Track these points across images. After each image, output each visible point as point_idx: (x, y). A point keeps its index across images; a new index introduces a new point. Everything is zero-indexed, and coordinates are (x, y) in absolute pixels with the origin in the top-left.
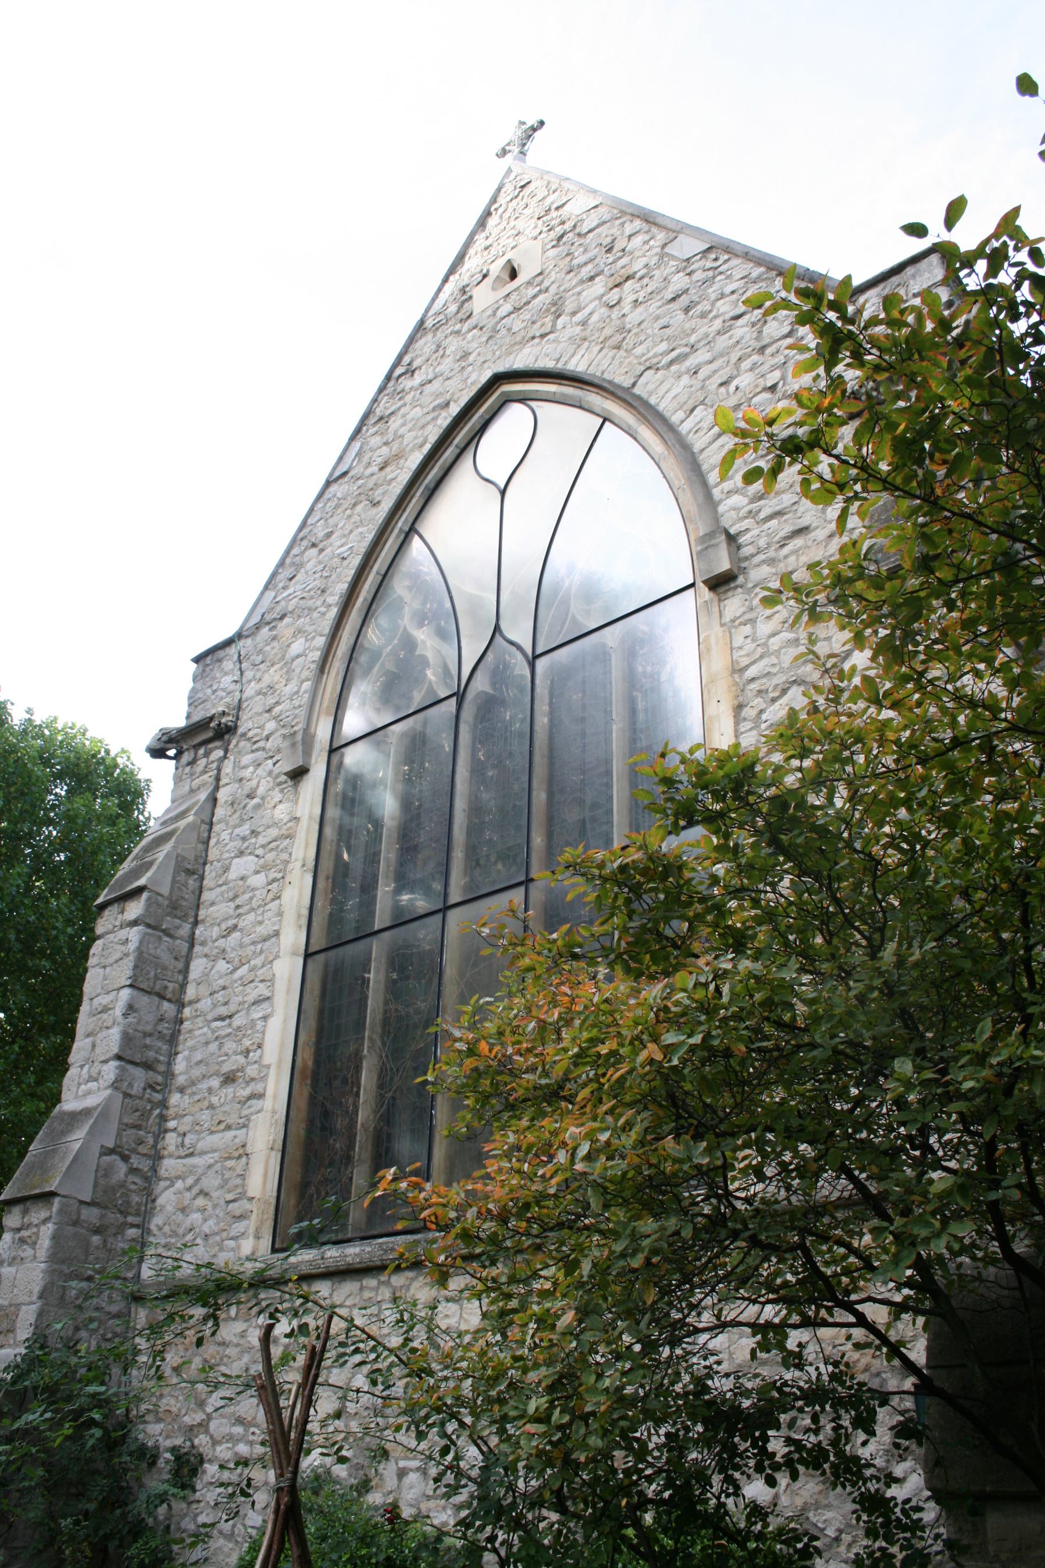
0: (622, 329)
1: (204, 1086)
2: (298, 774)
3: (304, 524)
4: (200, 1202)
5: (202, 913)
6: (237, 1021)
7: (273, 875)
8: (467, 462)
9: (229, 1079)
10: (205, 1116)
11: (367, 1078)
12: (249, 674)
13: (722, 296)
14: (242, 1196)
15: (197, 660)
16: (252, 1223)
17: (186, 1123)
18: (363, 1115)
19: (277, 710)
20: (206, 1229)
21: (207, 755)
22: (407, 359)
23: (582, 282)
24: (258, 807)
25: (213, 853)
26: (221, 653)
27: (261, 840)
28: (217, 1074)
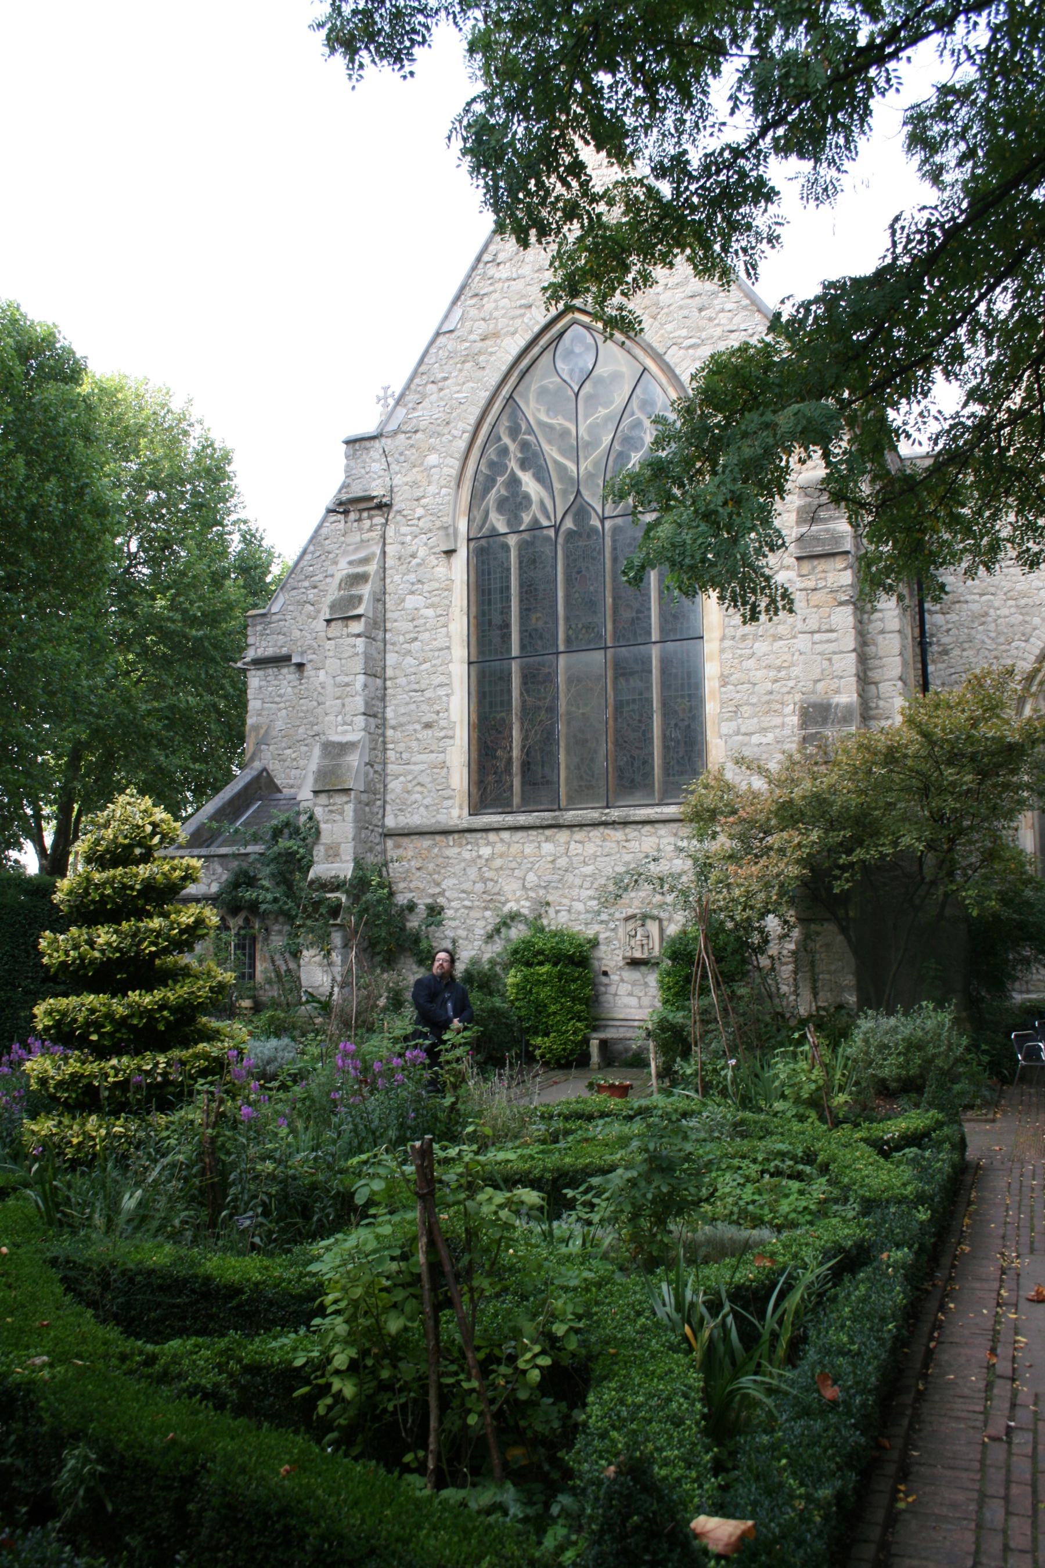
0: (656, 304)
1: (410, 727)
2: (450, 553)
3: (421, 362)
4: (419, 788)
5: (388, 625)
6: (428, 694)
7: (439, 612)
8: (547, 357)
9: (428, 726)
10: (414, 744)
11: (516, 733)
12: (394, 467)
13: (722, 310)
14: (448, 787)
15: (347, 442)
16: (457, 802)
17: (401, 747)
18: (516, 753)
19: (423, 501)
20: (426, 802)
21: (370, 518)
24: (419, 565)
25: (390, 588)
26: (367, 444)
27: (426, 588)
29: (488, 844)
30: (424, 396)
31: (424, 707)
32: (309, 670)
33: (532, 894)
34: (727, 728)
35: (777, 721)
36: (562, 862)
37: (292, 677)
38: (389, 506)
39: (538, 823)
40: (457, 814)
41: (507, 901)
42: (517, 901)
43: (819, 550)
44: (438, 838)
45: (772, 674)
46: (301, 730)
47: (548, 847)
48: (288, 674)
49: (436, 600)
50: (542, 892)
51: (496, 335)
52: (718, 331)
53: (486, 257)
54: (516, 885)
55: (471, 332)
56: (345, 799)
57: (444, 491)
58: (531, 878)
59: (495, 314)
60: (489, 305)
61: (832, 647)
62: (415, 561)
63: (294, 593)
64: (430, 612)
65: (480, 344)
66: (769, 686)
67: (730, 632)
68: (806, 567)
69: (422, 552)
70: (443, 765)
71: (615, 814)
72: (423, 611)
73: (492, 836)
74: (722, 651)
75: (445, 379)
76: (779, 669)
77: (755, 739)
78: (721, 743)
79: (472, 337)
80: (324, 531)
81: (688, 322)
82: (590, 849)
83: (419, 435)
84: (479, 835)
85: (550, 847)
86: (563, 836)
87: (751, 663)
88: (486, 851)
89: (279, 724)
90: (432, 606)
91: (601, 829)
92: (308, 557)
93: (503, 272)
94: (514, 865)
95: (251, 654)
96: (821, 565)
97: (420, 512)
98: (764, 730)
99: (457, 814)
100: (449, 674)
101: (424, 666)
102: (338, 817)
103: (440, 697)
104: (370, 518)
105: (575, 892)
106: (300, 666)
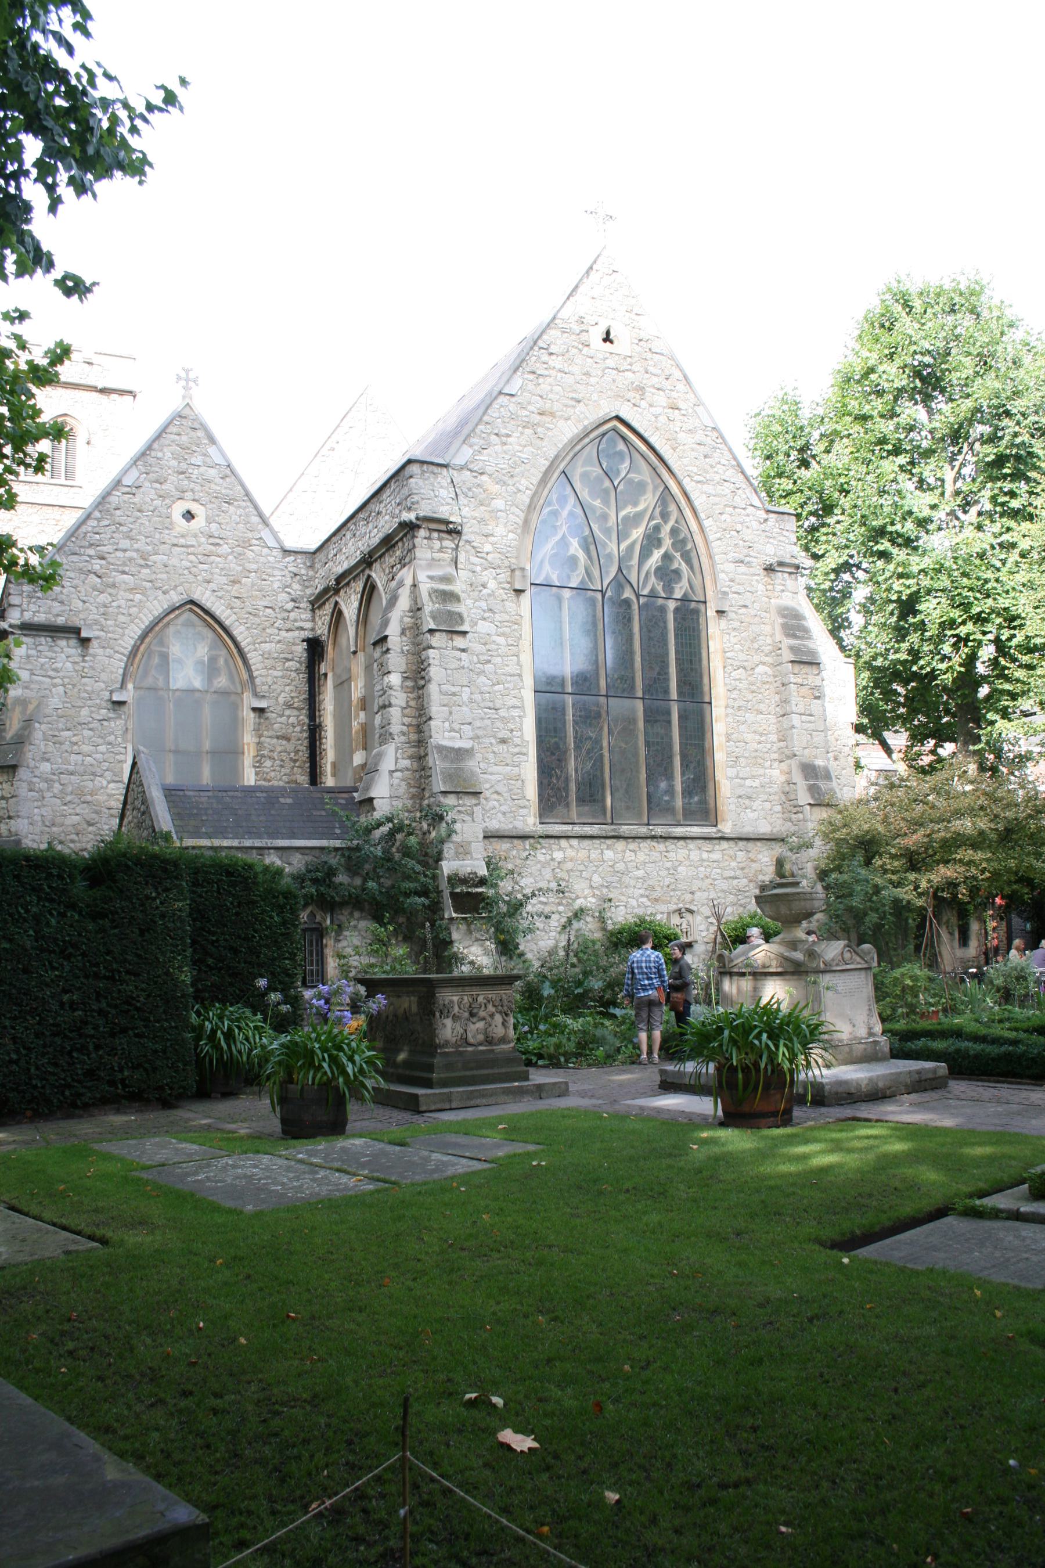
1: (487, 741)
4: (495, 796)
6: (503, 713)
9: (503, 741)
10: (491, 756)
22: (545, 337)
23: (653, 386)
24: (489, 595)
26: (436, 469)
27: (497, 617)
28: (495, 737)
29: (560, 849)
30: (489, 444)
31: (499, 724)
32: (94, 647)
33: (597, 892)
34: (732, 772)
35: (761, 771)
36: (620, 866)
37: (73, 651)
38: (459, 533)
39: (599, 833)
40: (529, 821)
41: (577, 897)
42: (585, 898)
43: (804, 658)
44: (516, 842)
45: (757, 737)
46: (85, 712)
47: (609, 854)
48: (67, 647)
49: (507, 630)
50: (605, 891)
51: (552, 414)
52: (717, 478)
53: (541, 343)
54: (584, 884)
55: (529, 403)
56: (474, 801)
57: (511, 536)
58: (596, 878)
59: (550, 396)
60: (544, 386)
61: (811, 726)
62: (485, 591)
63: (75, 558)
64: (501, 640)
65: (538, 417)
66: (756, 746)
67: (731, 702)
68: (797, 668)
69: (492, 585)
70: (518, 778)
71: (659, 830)
72: (495, 638)
73: (563, 843)
74: (727, 715)
75: (508, 436)
76: (761, 735)
77: (748, 782)
78: (727, 783)
79: (531, 408)
80: (114, 499)
81: (698, 463)
82: (641, 857)
83: (484, 478)
84: (552, 841)
85: (612, 853)
86: (620, 845)
87: (742, 728)
88: (558, 855)
89: (54, 702)
90: (503, 634)
91: (649, 841)
92: (92, 523)
93: (556, 362)
94: (581, 867)
95: (14, 617)
96: (806, 669)
97: (488, 548)
98: (753, 777)
99: (529, 821)
100: (521, 699)
101: (496, 688)
102: (467, 818)
103: (513, 718)
104: (440, 539)
105: (630, 891)
106: (87, 640)
